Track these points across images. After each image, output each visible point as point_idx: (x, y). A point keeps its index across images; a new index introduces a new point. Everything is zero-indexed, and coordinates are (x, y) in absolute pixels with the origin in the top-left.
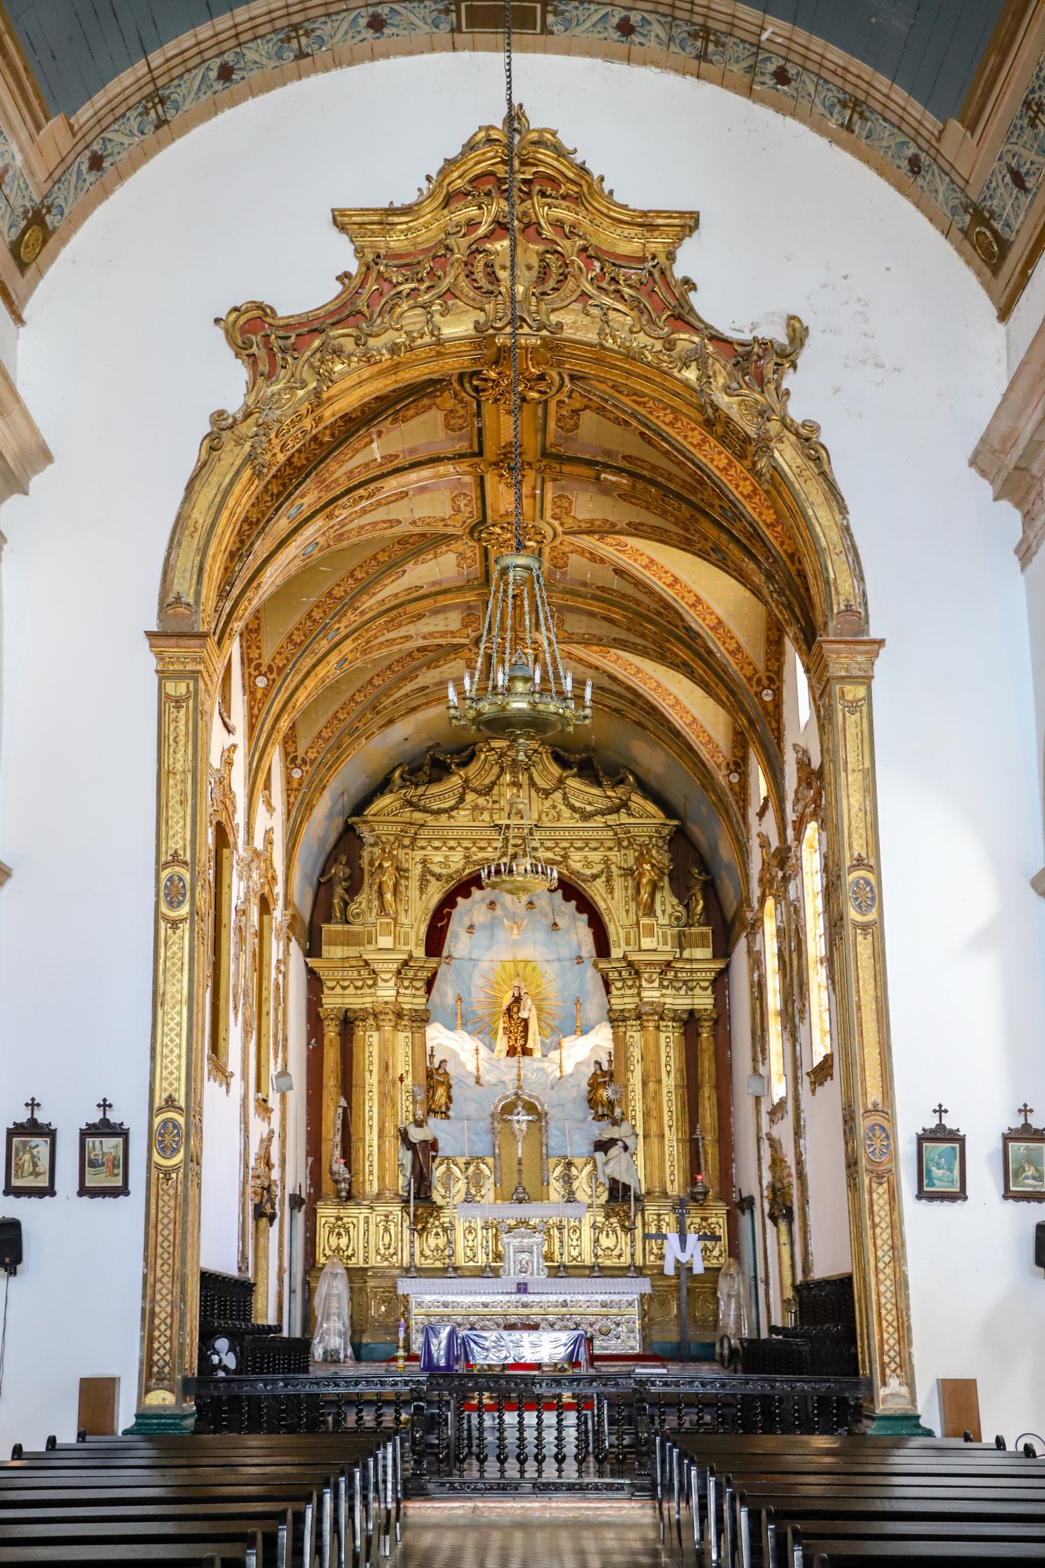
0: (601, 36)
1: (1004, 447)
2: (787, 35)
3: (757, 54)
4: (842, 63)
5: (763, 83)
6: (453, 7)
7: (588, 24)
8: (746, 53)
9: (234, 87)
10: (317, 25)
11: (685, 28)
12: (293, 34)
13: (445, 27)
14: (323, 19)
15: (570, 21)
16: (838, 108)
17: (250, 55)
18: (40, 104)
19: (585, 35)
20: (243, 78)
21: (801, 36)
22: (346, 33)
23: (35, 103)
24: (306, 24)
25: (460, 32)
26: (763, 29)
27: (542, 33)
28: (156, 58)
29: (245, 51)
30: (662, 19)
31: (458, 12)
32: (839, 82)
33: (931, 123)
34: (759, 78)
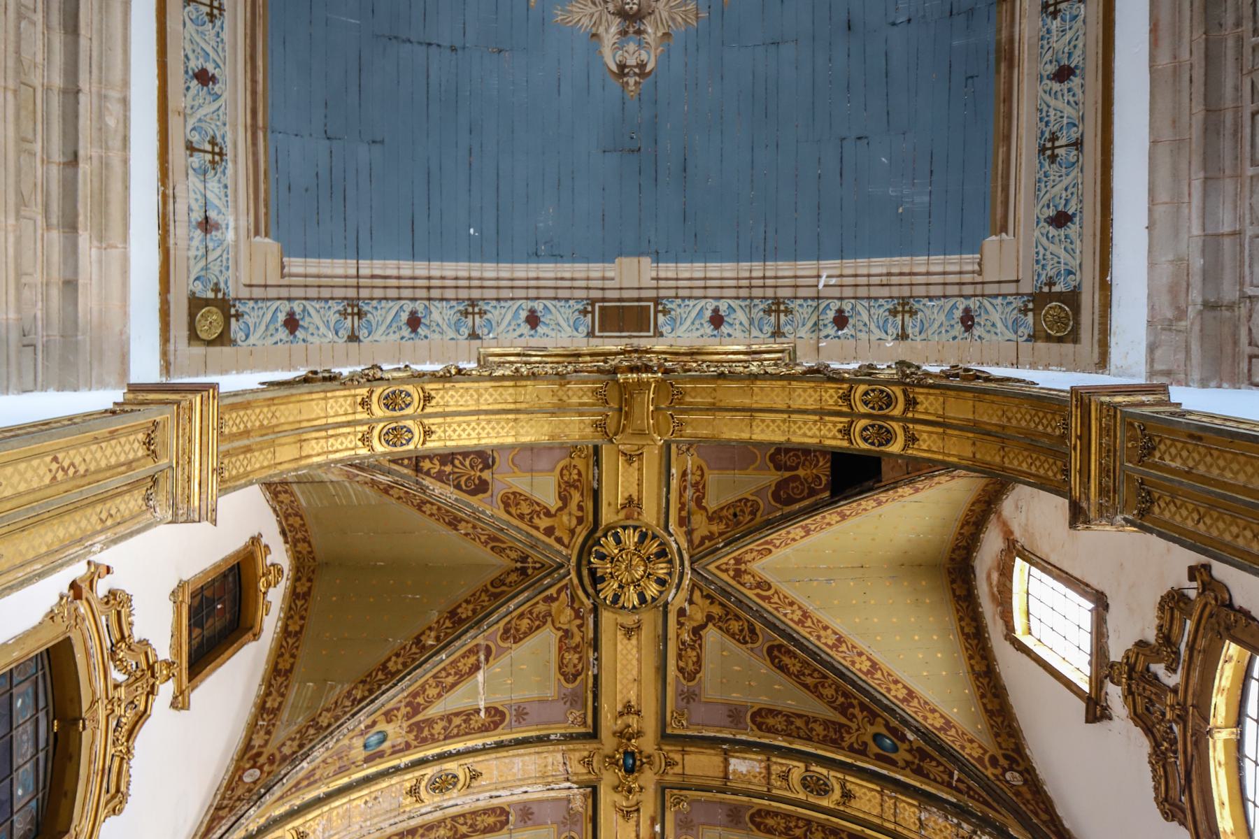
0: (699, 333)
1: (1178, 308)
2: (837, 272)
3: (817, 307)
4: (884, 271)
5: (827, 337)
6: (589, 308)
7: (689, 322)
8: (810, 310)
9: (417, 342)
10: (488, 308)
11: (761, 307)
12: (470, 310)
13: (583, 330)
14: (494, 303)
15: (674, 320)
16: (891, 318)
17: (436, 316)
18: (266, 214)
19: (687, 335)
20: (426, 337)
21: (849, 266)
22: (509, 324)
23: (262, 210)
24: (480, 303)
25: (594, 336)
26: (819, 277)
27: (654, 336)
28: (366, 267)
29: (433, 309)
30: (743, 304)
31: (593, 312)
32: (885, 292)
33: (968, 262)
34: (823, 334)
